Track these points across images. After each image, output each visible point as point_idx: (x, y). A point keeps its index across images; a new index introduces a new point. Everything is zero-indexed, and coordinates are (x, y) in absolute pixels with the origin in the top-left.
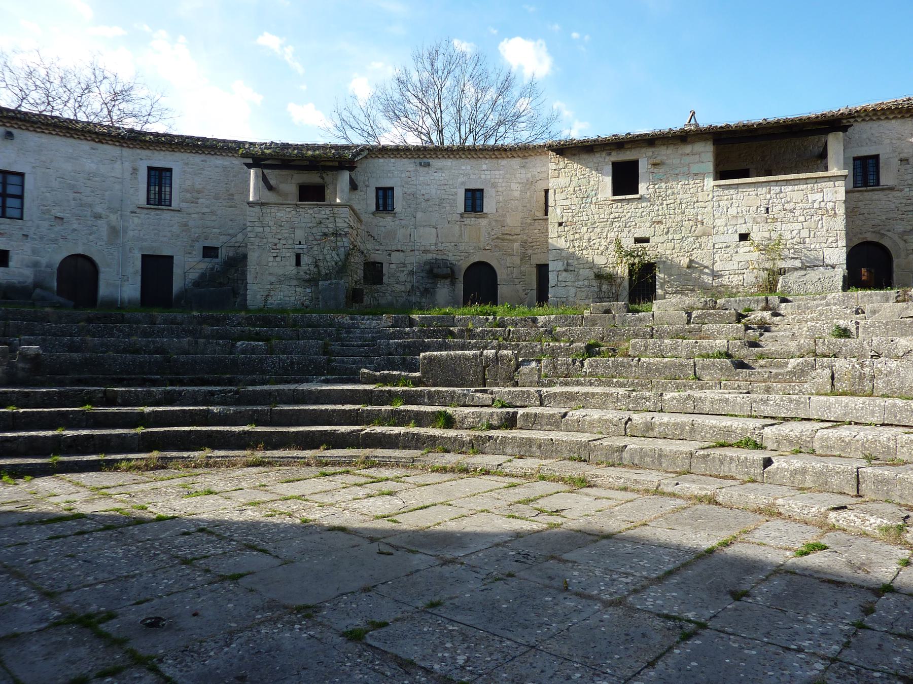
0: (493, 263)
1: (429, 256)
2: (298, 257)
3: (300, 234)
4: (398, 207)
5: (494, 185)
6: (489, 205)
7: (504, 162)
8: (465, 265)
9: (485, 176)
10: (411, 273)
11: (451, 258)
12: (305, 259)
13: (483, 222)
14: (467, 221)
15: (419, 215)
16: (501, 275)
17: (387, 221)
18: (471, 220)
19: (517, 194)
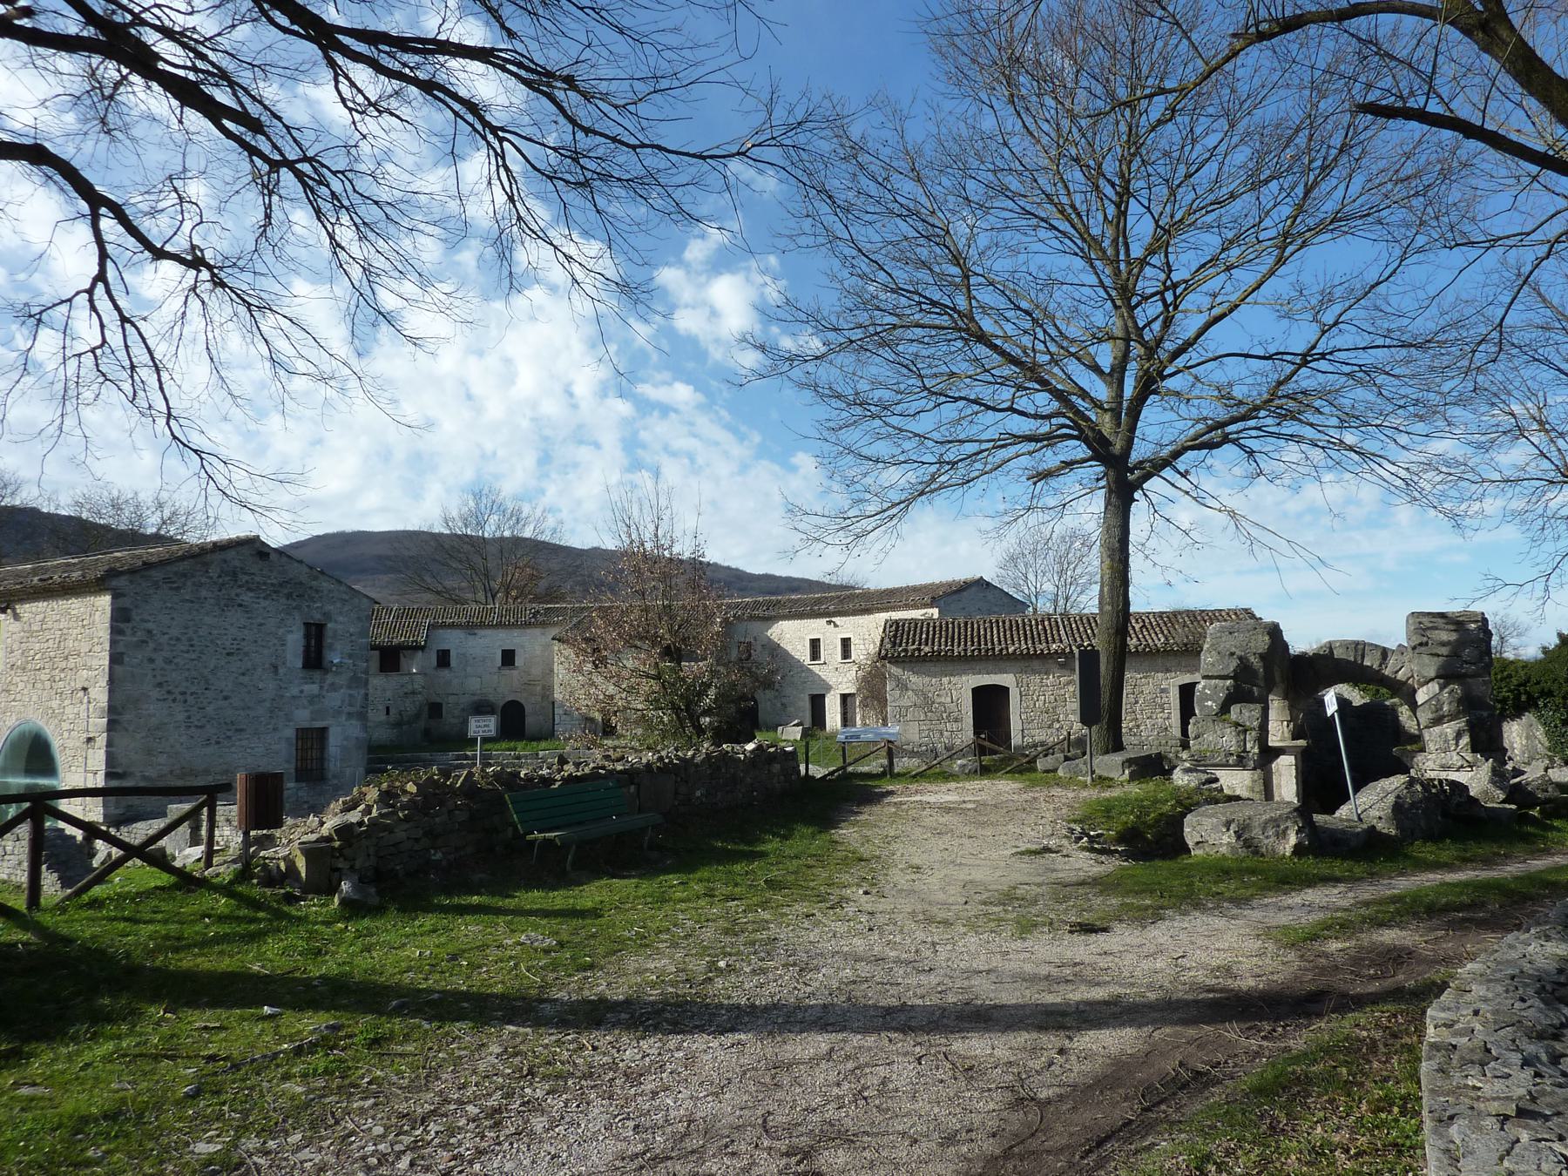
0: (522, 701)
1: (476, 698)
2: (388, 708)
3: (389, 694)
4: (453, 663)
5: (523, 647)
6: (519, 661)
7: (528, 631)
8: (501, 703)
9: (517, 640)
10: (463, 710)
11: (491, 698)
12: (392, 711)
13: (515, 672)
14: (503, 672)
15: (469, 669)
16: (528, 709)
17: (445, 673)
18: (506, 672)
19: (538, 652)
